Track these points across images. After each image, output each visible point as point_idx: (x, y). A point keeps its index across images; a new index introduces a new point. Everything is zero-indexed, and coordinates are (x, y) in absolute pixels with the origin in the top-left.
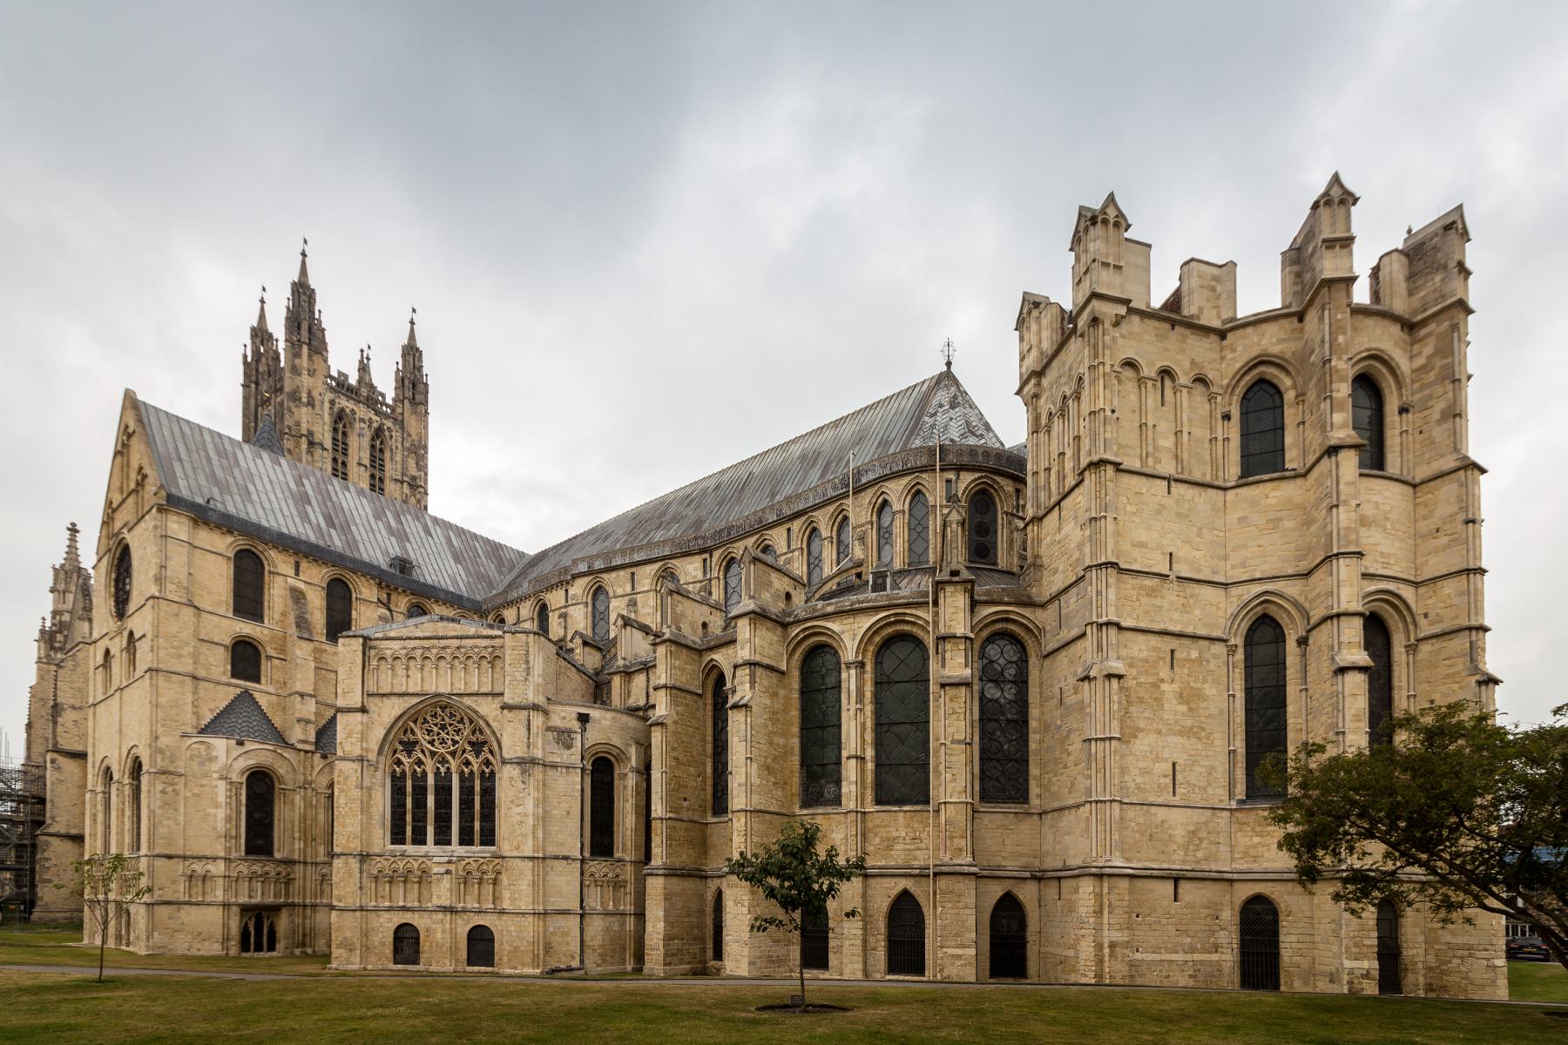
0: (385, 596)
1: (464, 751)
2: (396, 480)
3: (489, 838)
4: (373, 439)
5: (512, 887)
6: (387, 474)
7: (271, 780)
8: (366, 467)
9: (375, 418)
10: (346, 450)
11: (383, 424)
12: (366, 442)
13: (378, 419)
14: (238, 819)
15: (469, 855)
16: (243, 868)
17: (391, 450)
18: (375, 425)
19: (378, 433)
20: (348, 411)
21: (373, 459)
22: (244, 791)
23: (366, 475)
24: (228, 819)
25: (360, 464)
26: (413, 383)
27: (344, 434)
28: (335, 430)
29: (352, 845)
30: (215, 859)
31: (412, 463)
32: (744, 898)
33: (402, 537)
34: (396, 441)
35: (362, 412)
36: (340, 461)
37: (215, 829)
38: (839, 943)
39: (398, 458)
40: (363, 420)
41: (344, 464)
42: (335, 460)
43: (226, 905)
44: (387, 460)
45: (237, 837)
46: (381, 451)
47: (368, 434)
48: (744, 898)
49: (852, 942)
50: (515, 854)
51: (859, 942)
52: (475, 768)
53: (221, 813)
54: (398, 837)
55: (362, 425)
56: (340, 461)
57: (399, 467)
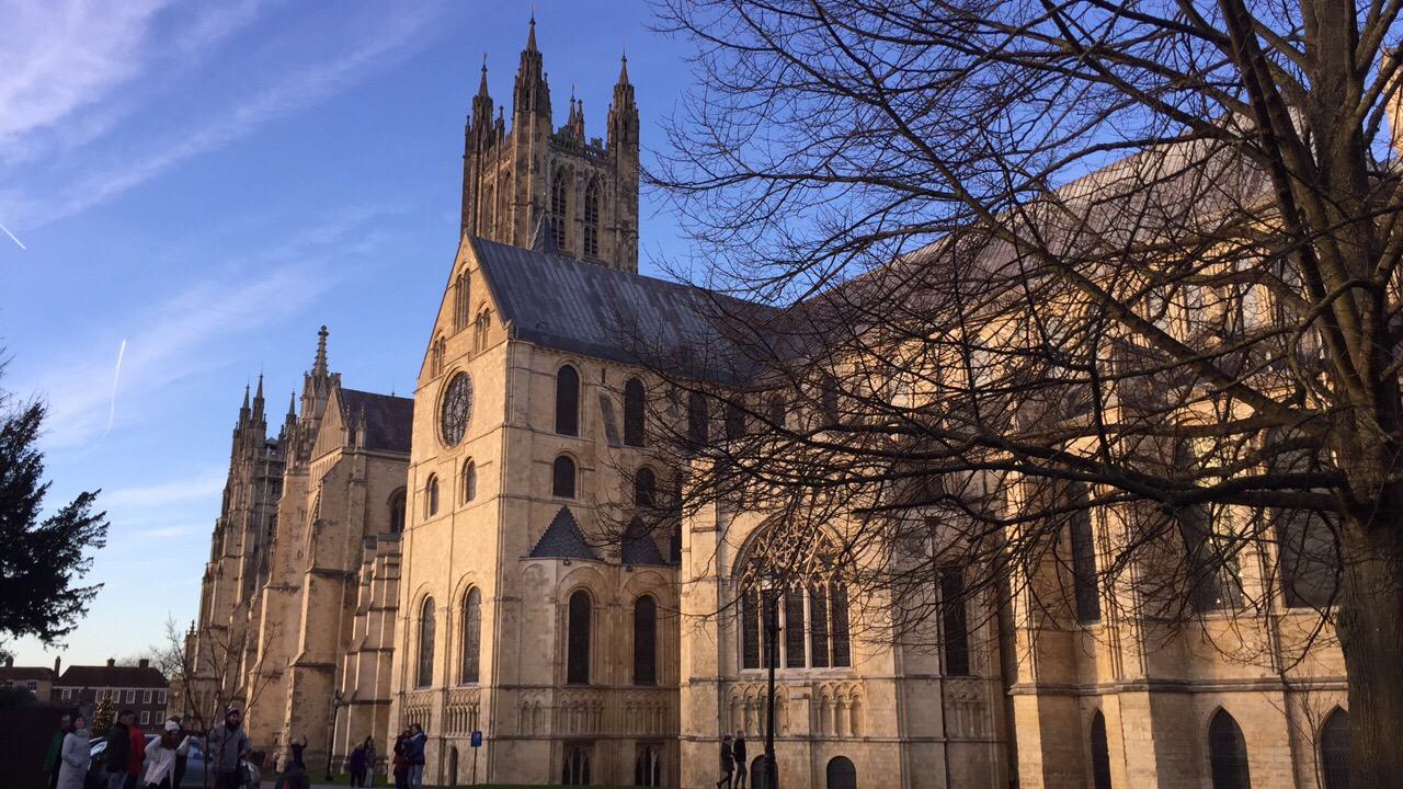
1: (814, 565)
2: (609, 229)
3: (842, 658)
4: (588, 190)
5: (875, 713)
6: (600, 223)
7: (588, 600)
10: (564, 207)
12: (582, 196)
13: (593, 168)
14: (563, 645)
15: (825, 677)
16: (566, 698)
17: (605, 197)
18: (591, 175)
19: (592, 184)
20: (567, 167)
24: (556, 644)
25: (576, 220)
26: (626, 124)
29: (710, 670)
30: (544, 688)
31: (624, 207)
32: (1144, 720)
34: (610, 187)
35: (580, 165)
36: (558, 220)
37: (545, 656)
38: (1263, 774)
39: (612, 205)
40: (579, 174)
41: (562, 223)
43: (553, 739)
44: (600, 209)
45: (562, 664)
47: (584, 186)
48: (1144, 720)
49: (1280, 772)
50: (876, 674)
51: (1289, 772)
52: (826, 583)
53: (551, 639)
54: (749, 660)
55: (580, 179)
56: (558, 220)
57: (612, 214)
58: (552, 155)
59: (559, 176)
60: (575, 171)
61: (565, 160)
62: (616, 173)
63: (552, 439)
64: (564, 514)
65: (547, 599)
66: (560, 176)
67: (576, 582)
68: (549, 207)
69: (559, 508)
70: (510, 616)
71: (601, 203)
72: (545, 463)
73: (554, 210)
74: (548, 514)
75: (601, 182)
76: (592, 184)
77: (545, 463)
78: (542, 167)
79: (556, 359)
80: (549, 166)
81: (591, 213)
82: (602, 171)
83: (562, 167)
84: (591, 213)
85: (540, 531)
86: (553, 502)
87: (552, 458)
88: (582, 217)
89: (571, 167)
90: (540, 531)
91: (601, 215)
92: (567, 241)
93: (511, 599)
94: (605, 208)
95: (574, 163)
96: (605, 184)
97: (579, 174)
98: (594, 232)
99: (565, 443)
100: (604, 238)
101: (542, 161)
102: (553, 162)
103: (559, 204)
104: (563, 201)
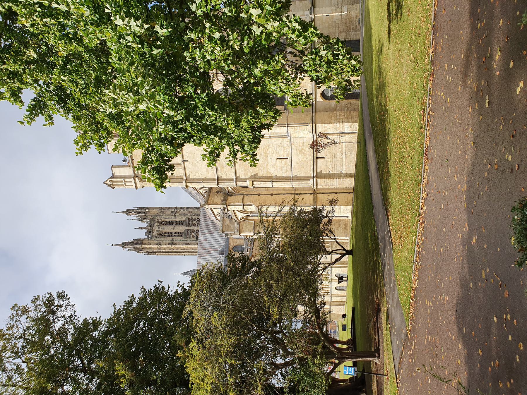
18: (158, 224)
19: (161, 223)
27: (165, 233)
28: (165, 236)
35: (156, 229)
40: (159, 228)
41: (175, 233)
42: (175, 236)
46: (166, 222)
47: (162, 226)
55: (160, 228)
58: (154, 238)
59: (160, 234)
61: (155, 233)
66: (161, 235)
68: (171, 238)
71: (167, 220)
75: (160, 220)
78: (159, 242)
80: (158, 239)
81: (171, 223)
82: (156, 220)
84: (171, 223)
91: (171, 220)
92: (181, 231)
95: (155, 230)
97: (159, 228)
98: (176, 222)
100: (178, 219)
101: (157, 242)
103: (169, 234)
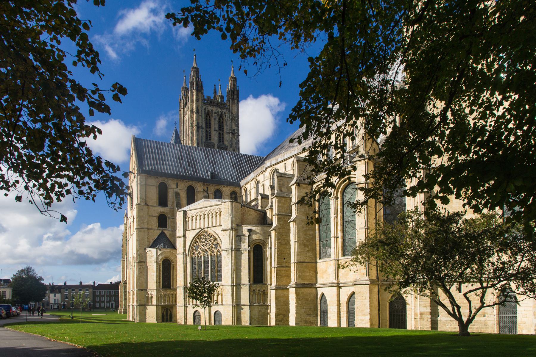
0: (206, 188)
8: (217, 131)
9: (220, 110)
11: (223, 112)
13: (221, 110)
18: (220, 113)
21: (219, 127)
22: (161, 266)
23: (217, 134)
27: (210, 120)
28: (206, 119)
33: (214, 163)
35: (215, 109)
40: (215, 113)
42: (206, 131)
46: (223, 122)
47: (217, 117)
55: (215, 115)
58: (204, 107)
59: (208, 114)
60: (214, 112)
61: (210, 108)
62: (229, 111)
63: (156, 208)
64: (162, 234)
65: (153, 262)
67: (163, 256)
68: (204, 126)
69: (160, 231)
70: (142, 268)
72: (154, 216)
73: (206, 127)
74: (156, 234)
75: (224, 115)
76: (221, 117)
77: (154, 216)
78: (200, 111)
79: (157, 180)
80: (203, 111)
82: (224, 111)
83: (209, 111)
85: (153, 240)
86: (158, 230)
87: (157, 215)
88: (217, 129)
89: (212, 110)
90: (153, 240)
91: (225, 128)
93: (142, 262)
94: (226, 125)
95: (213, 109)
96: (226, 116)
97: (215, 113)
99: (162, 210)
101: (200, 109)
102: (205, 109)
104: (210, 124)
